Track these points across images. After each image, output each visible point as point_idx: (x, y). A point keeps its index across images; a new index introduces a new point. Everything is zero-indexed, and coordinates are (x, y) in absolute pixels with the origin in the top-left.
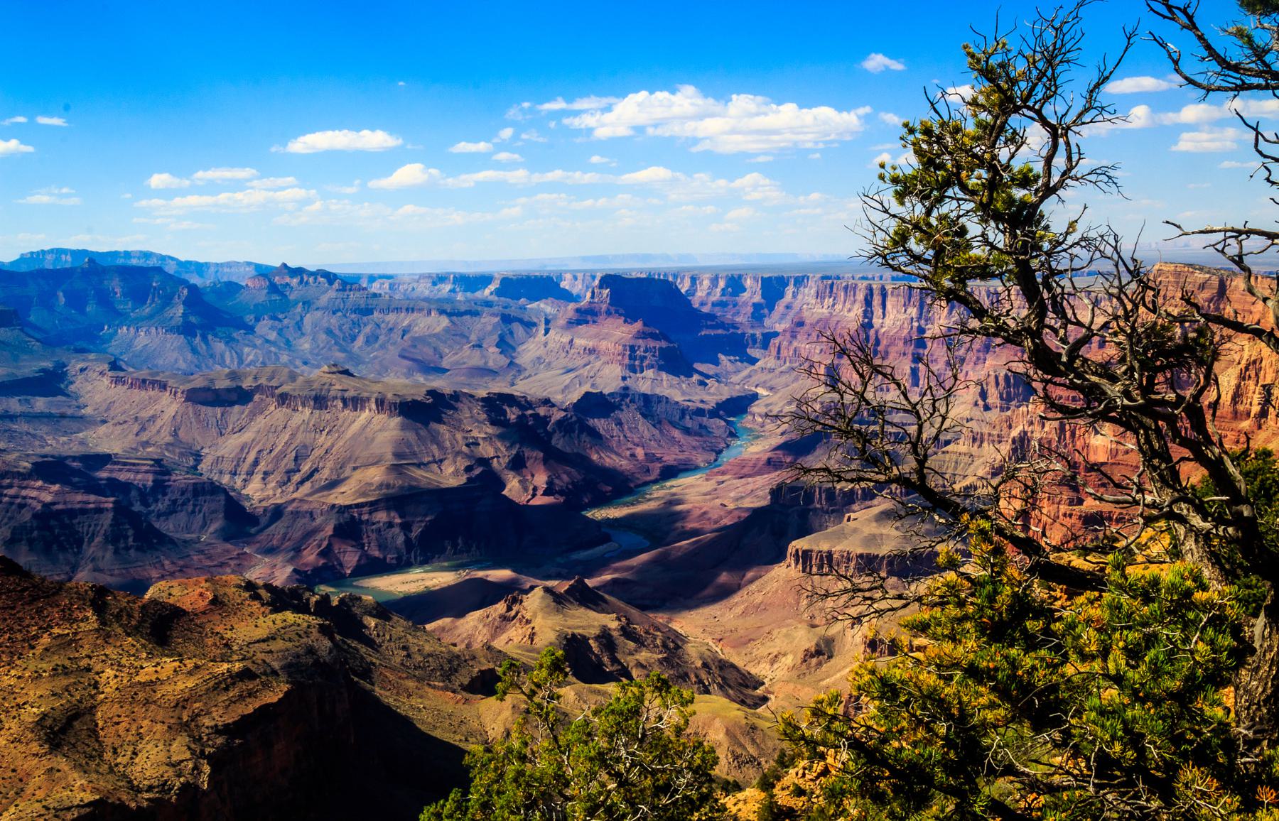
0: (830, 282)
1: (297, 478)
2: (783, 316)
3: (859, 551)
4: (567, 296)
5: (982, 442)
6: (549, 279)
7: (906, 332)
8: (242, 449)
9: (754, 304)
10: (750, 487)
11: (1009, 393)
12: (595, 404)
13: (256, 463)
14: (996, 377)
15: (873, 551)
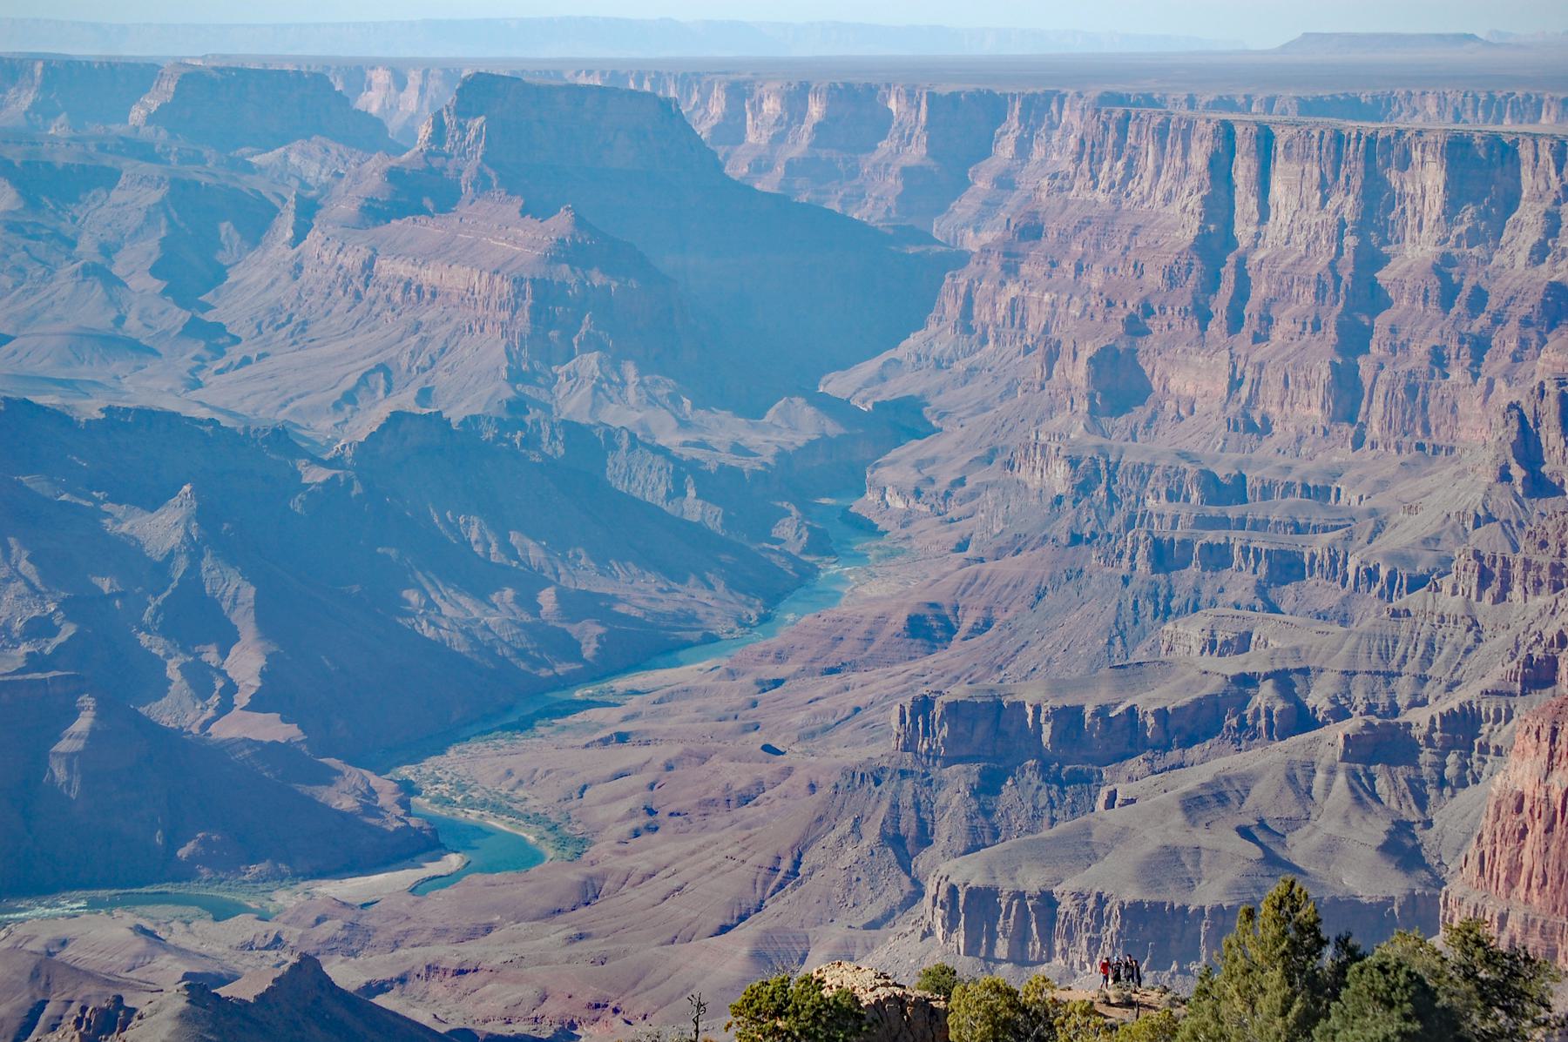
0: (1118, 112)
2: (990, 206)
3: (1131, 895)
4: (368, 133)
5: (1506, 587)
7: (1322, 262)
9: (905, 172)
10: (852, 699)
12: (424, 446)
15: (1173, 896)
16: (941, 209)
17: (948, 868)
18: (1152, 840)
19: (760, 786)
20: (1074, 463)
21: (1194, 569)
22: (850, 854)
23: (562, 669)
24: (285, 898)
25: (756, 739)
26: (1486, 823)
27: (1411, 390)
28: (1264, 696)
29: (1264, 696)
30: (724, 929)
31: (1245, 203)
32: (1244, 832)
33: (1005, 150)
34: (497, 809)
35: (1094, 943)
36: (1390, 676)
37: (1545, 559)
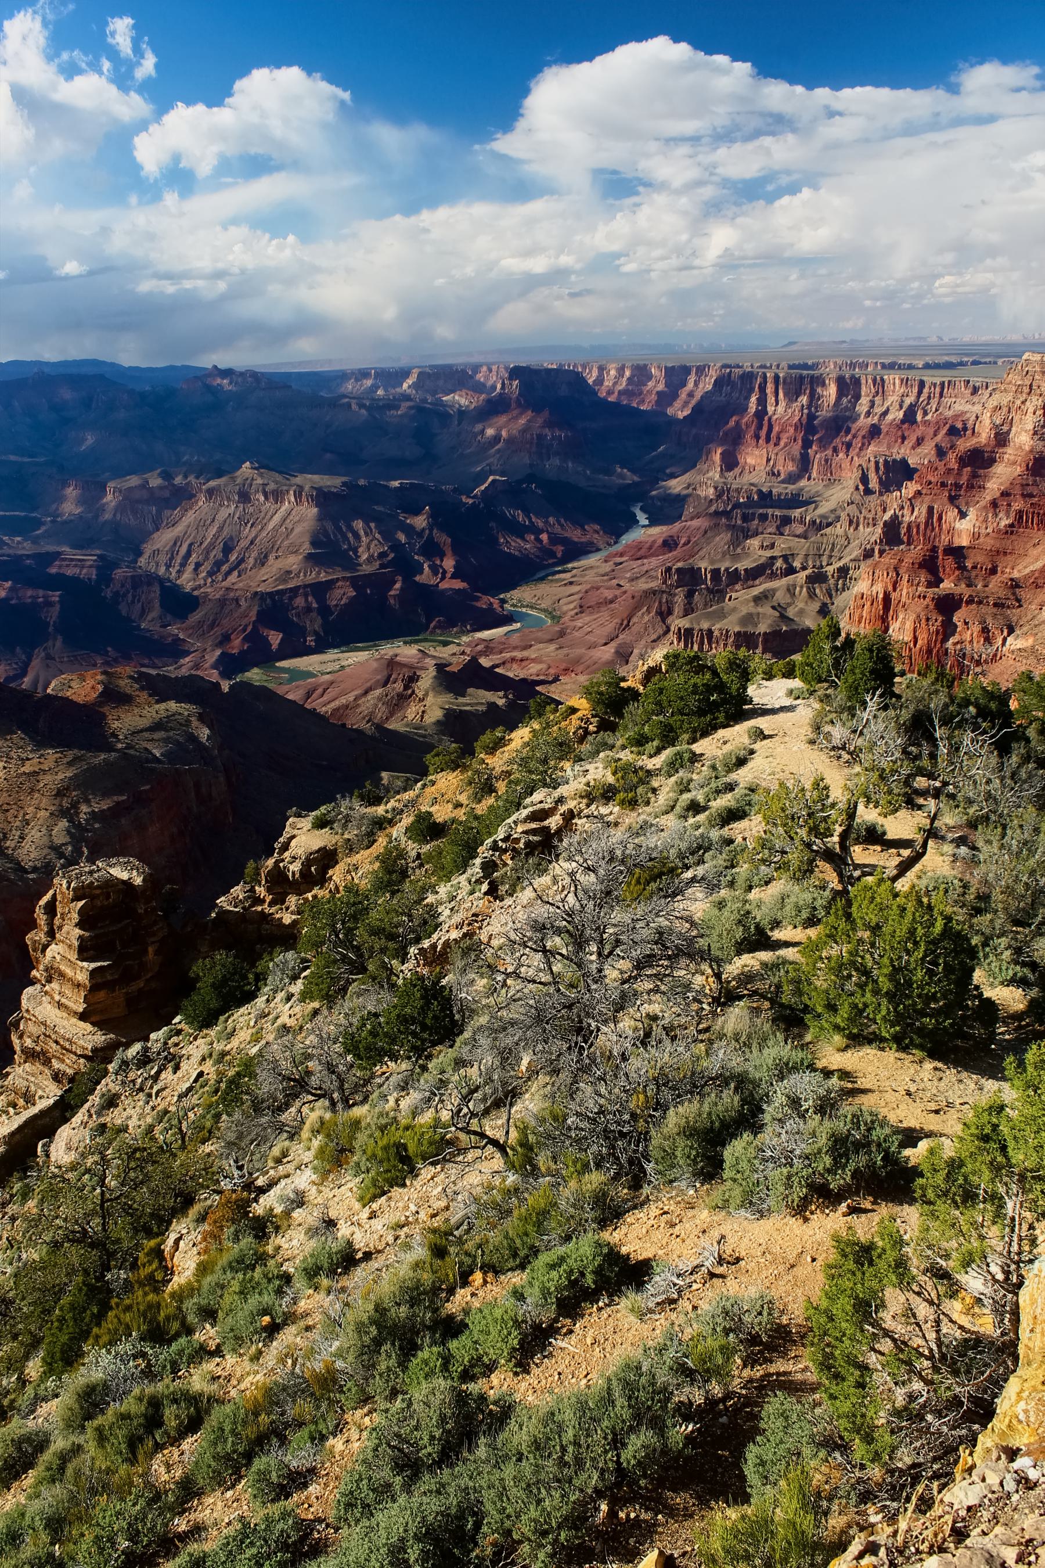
1: (225, 568)
2: (686, 403)
3: (737, 629)
4: (479, 388)
5: (858, 525)
6: (464, 372)
7: (797, 418)
8: (175, 543)
10: (645, 568)
11: (887, 477)
13: (189, 554)
14: (877, 463)
15: (750, 629)
16: (670, 404)
17: (678, 622)
18: (744, 611)
19: (616, 597)
20: (716, 488)
21: (756, 522)
22: (646, 618)
23: (551, 561)
24: (465, 639)
25: (615, 582)
26: (852, 603)
27: (826, 461)
28: (779, 563)
29: (779, 563)
30: (606, 644)
31: (771, 399)
32: (773, 608)
33: (690, 385)
34: (532, 607)
35: (725, 645)
36: (820, 556)
37: (870, 516)
